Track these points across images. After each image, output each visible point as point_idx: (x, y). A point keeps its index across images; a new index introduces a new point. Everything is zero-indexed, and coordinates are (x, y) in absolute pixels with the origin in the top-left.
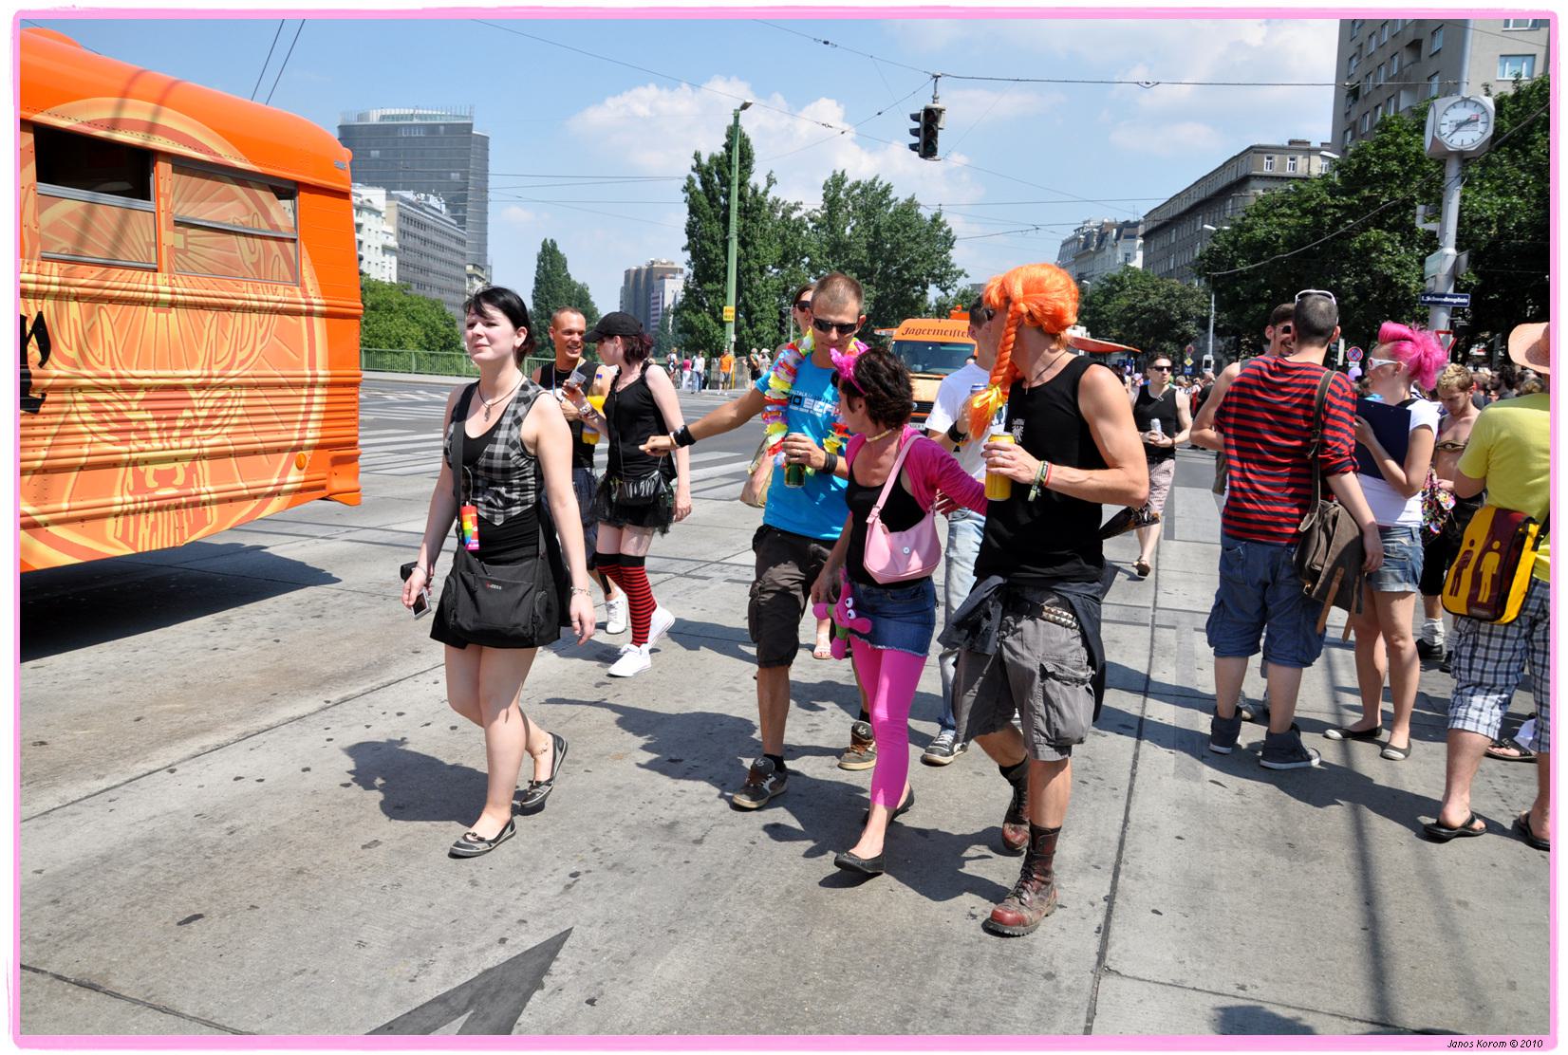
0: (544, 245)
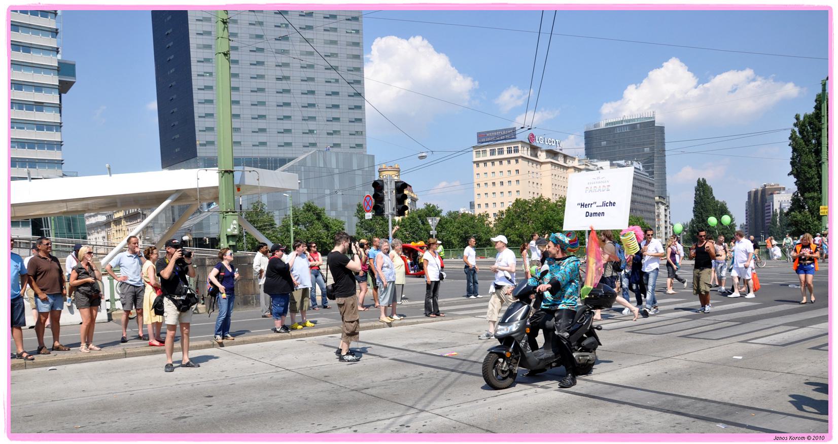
0: (699, 181)
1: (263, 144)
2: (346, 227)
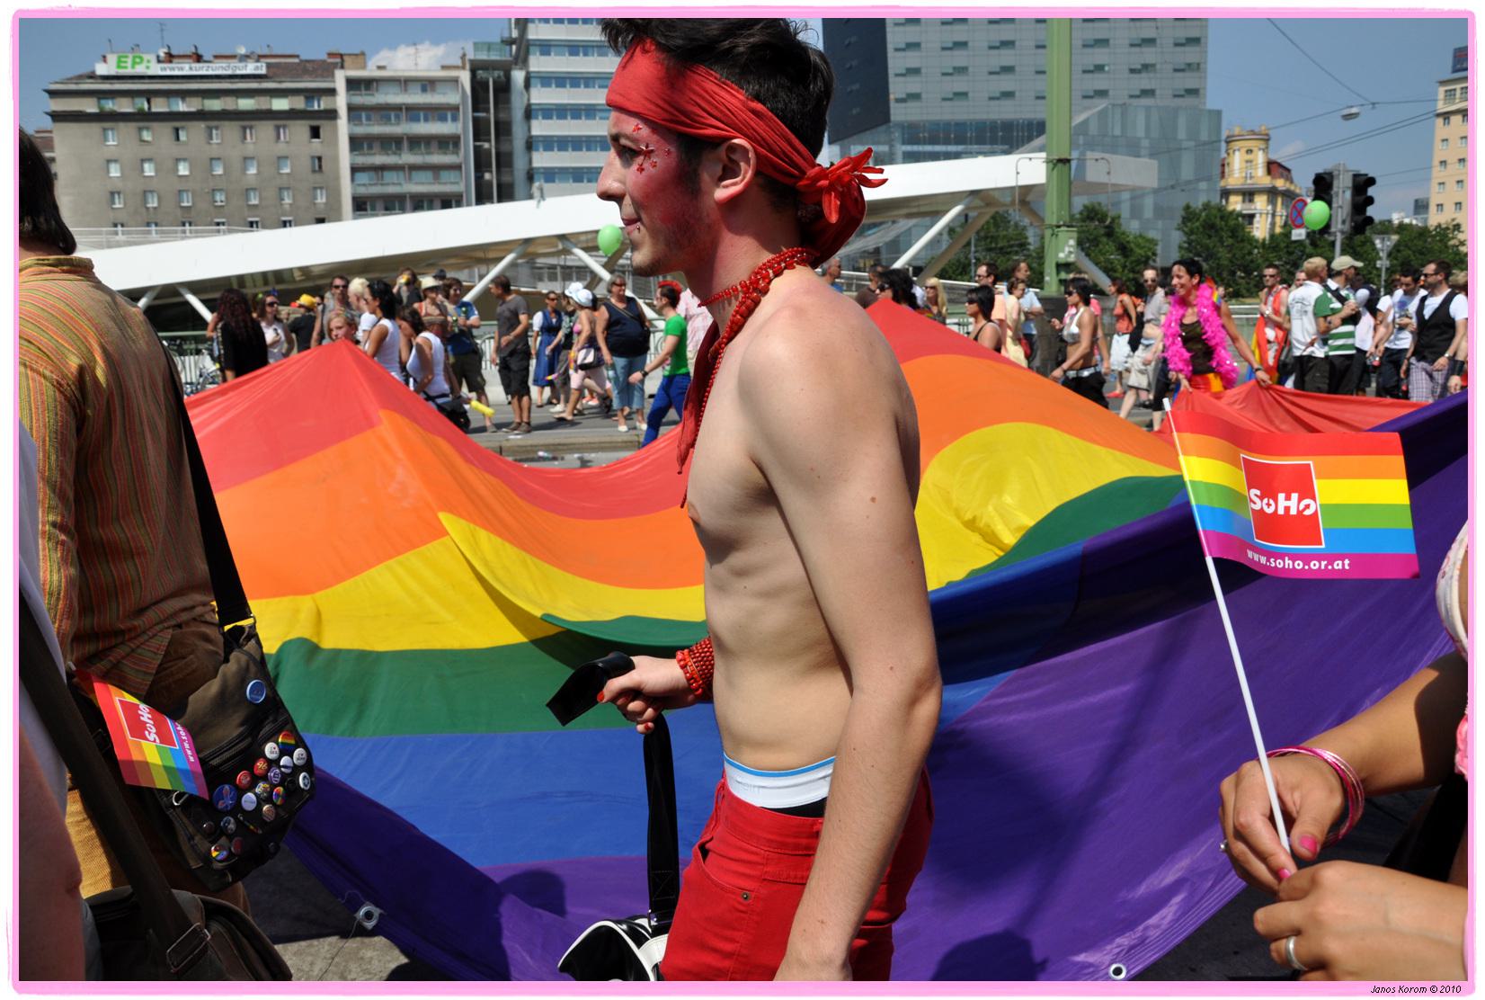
1: (1008, 95)
2: (1159, 249)
